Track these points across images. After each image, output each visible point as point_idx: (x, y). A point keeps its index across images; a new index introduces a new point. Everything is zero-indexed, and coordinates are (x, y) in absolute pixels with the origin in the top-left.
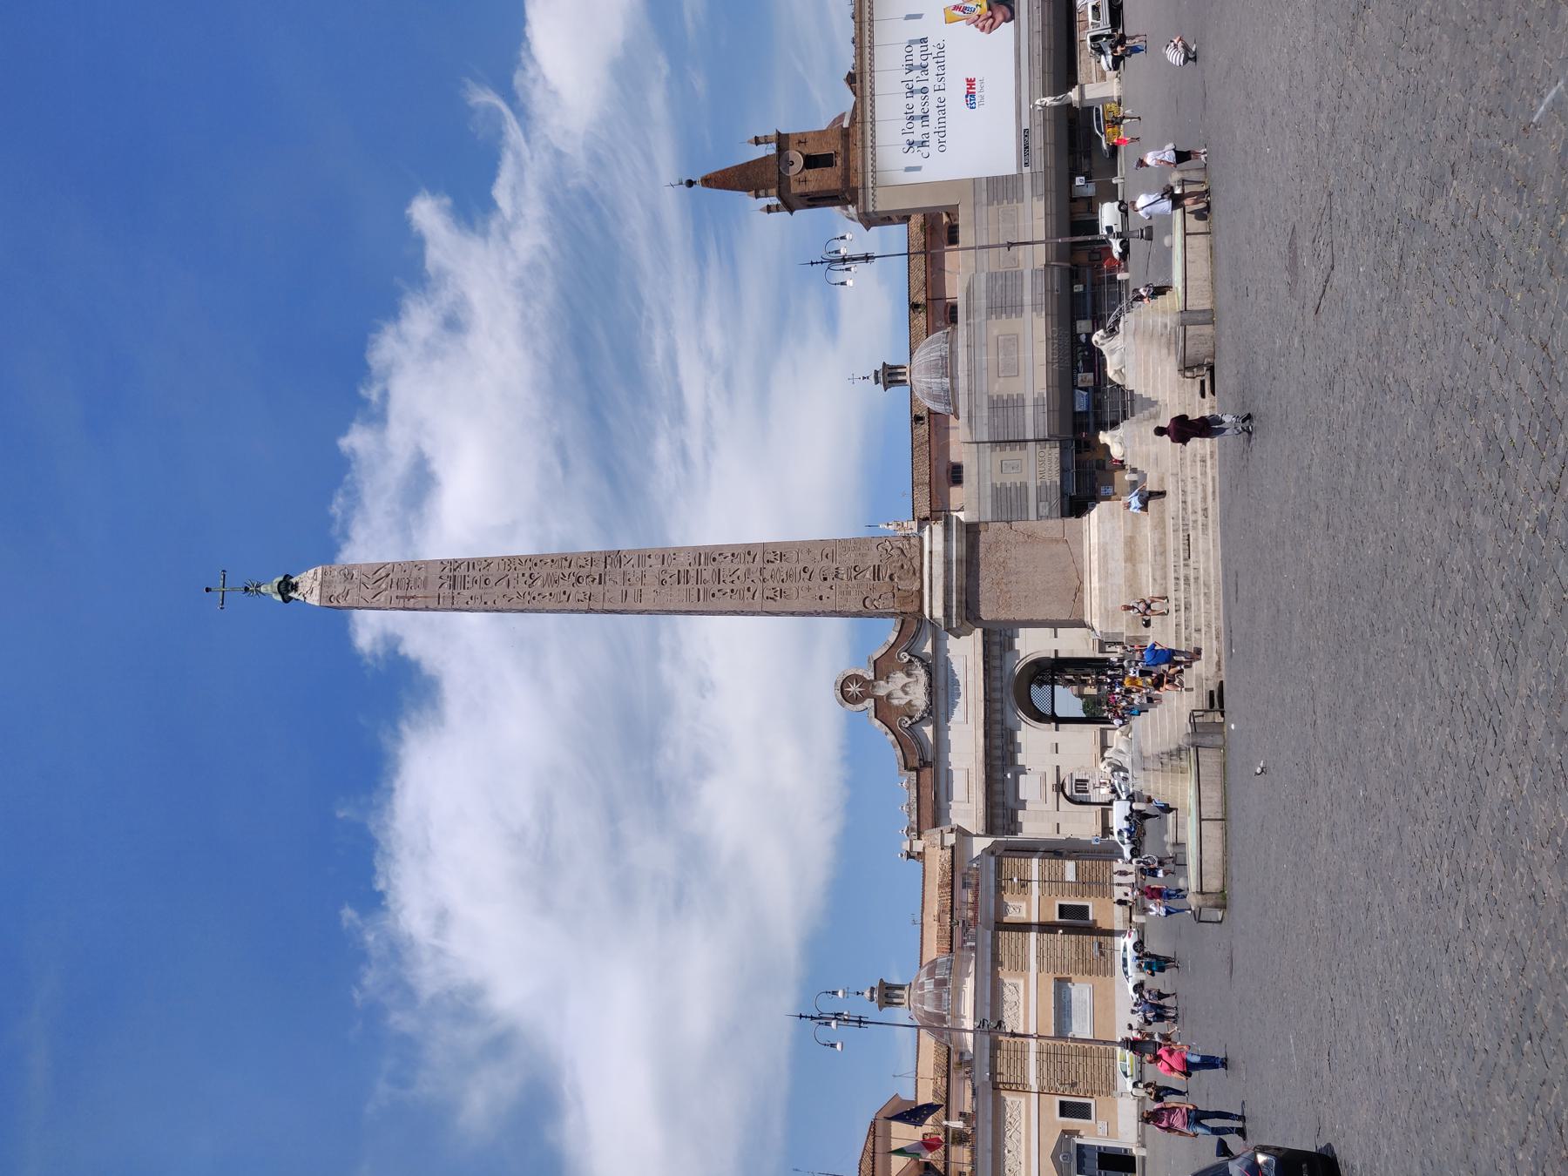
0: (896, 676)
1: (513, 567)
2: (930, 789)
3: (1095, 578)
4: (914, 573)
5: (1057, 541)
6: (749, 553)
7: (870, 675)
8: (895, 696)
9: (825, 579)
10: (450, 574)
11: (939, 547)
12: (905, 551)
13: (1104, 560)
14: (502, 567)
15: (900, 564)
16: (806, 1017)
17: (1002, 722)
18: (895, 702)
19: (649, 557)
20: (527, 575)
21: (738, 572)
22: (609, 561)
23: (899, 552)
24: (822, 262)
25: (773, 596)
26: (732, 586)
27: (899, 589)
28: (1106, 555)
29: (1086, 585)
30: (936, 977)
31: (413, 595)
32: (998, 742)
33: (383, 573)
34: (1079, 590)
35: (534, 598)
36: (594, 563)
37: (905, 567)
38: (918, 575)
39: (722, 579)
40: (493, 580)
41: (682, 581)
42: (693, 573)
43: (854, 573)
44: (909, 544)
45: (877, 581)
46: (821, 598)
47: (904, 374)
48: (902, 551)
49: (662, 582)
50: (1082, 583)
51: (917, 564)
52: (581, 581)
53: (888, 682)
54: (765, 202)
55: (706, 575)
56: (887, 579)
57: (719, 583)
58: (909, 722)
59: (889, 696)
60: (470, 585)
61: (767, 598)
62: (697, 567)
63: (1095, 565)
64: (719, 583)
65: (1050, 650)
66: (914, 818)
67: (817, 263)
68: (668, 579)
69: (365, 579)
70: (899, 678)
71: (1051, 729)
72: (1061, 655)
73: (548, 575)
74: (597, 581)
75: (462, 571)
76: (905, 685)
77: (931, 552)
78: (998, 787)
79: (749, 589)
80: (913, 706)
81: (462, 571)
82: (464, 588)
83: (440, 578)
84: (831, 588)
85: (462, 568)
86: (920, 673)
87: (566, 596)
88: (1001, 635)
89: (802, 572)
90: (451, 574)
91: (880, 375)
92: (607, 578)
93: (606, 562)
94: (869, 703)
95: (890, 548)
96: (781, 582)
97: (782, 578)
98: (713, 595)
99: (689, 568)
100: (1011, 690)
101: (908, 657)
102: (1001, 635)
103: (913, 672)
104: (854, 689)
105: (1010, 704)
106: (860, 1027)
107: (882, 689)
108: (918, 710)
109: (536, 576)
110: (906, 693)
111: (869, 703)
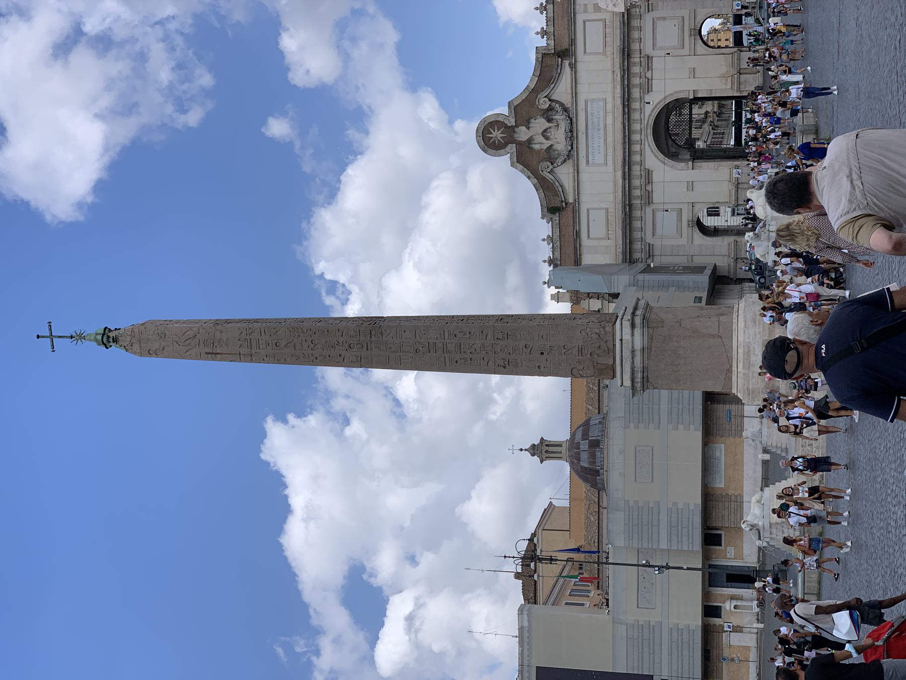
0: (537, 121)
1: (297, 334)
2: (572, 228)
3: (741, 365)
5: (714, 336)
7: (512, 122)
8: (536, 141)
9: (542, 354)
10: (246, 337)
11: (627, 336)
12: (601, 336)
13: (748, 353)
17: (641, 163)
18: (537, 147)
21: (475, 346)
22: (373, 333)
23: (596, 336)
26: (471, 356)
27: (597, 363)
28: (749, 351)
29: (734, 368)
30: (590, 438)
31: (218, 352)
32: (636, 182)
33: (190, 333)
34: (729, 371)
38: (611, 354)
40: (284, 343)
41: (432, 351)
42: (440, 345)
44: (605, 331)
46: (539, 367)
50: (731, 366)
52: (352, 347)
53: (528, 128)
55: (451, 347)
56: (589, 356)
58: (551, 167)
59: (530, 141)
60: (264, 346)
63: (741, 356)
65: (689, 91)
68: (420, 348)
69: (176, 338)
70: (539, 124)
71: (688, 169)
72: (700, 95)
74: (365, 346)
76: (545, 131)
77: (621, 340)
78: (637, 224)
80: (555, 150)
83: (239, 340)
86: (559, 117)
88: (641, 77)
89: (524, 348)
92: (373, 346)
93: (371, 334)
94: (512, 148)
95: (591, 333)
100: (650, 131)
101: (548, 103)
102: (641, 77)
103: (553, 117)
104: (497, 134)
105: (649, 145)
106: (551, 563)
107: (523, 134)
108: (559, 155)
109: (317, 342)
110: (547, 138)
111: (512, 148)
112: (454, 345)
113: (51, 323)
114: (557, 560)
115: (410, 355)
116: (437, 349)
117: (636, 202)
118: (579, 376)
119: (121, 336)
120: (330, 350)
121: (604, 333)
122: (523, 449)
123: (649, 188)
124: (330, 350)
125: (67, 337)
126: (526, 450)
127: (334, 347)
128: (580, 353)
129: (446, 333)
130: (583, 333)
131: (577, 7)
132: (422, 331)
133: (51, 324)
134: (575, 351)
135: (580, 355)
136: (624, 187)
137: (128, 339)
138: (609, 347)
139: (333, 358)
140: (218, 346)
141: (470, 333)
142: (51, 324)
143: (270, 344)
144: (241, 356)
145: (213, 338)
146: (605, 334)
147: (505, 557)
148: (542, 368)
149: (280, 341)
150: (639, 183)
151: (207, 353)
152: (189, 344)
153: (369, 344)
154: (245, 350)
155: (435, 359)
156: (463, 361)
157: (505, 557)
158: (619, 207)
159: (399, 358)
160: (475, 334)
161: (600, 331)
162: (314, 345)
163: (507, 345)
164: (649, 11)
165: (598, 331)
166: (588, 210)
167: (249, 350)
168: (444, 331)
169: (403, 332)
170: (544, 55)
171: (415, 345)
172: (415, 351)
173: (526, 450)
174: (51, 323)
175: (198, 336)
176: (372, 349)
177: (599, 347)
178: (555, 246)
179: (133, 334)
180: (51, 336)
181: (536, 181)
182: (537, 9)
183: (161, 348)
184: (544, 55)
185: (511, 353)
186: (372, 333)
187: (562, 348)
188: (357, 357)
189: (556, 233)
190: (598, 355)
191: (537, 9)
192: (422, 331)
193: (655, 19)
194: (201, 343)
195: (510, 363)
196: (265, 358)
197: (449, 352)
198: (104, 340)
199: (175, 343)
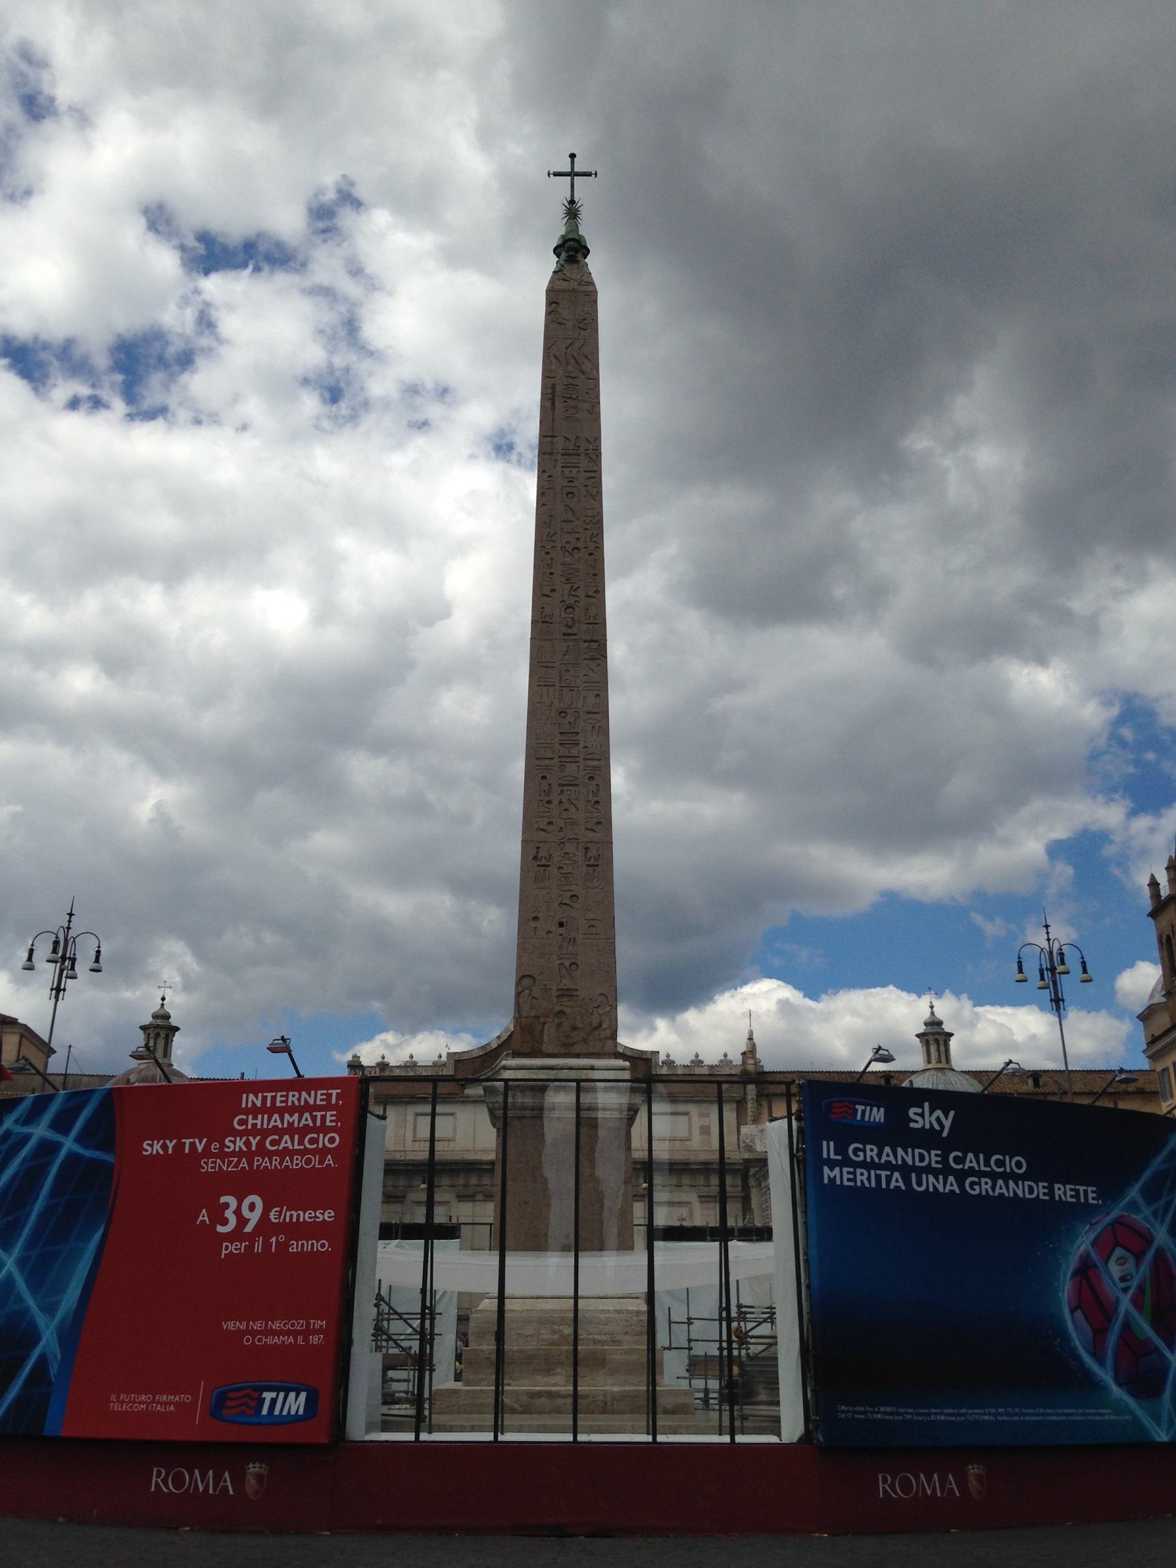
1: (588, 527)
4: (565, 1045)
6: (598, 823)
12: (596, 1033)
14: (589, 513)
15: (579, 1025)
16: (70, 921)
19: (597, 695)
20: (580, 545)
21: (573, 810)
22: (594, 645)
23: (595, 1022)
24: (1049, 940)
25: (540, 855)
26: (556, 802)
27: (544, 1024)
31: (557, 404)
33: (587, 366)
35: (547, 553)
36: (591, 626)
37: (575, 1033)
38: (562, 1051)
39: (565, 788)
42: (574, 752)
43: (567, 964)
44: (606, 1038)
45: (556, 994)
46: (536, 918)
47: (940, 1062)
48: (597, 1028)
49: (562, 713)
51: (576, 1049)
52: (568, 611)
54: (1163, 879)
55: (571, 769)
56: (558, 1008)
57: (560, 785)
61: (538, 848)
62: (582, 756)
64: (560, 785)
66: (397, 1073)
67: (1048, 933)
68: (569, 719)
73: (577, 570)
74: (570, 631)
75: (584, 463)
79: (550, 823)
81: (584, 463)
82: (562, 467)
83: (577, 437)
84: (549, 932)
85: (590, 464)
87: (548, 593)
89: (573, 893)
90: (582, 450)
91: (936, 1029)
92: (571, 644)
93: (592, 641)
96: (558, 865)
97: (564, 867)
98: (544, 778)
99: (581, 746)
106: (52, 990)
112: (575, 774)
113: (596, 176)
114: (57, 998)
115: (556, 702)
116: (567, 746)
117: (461, 1181)
118: (520, 989)
119: (578, 268)
120: (562, 575)
121: (602, 1036)
122: (164, 1002)
123: (480, 1197)
124: (562, 575)
125: (572, 195)
126: (162, 1005)
127: (568, 582)
128: (565, 992)
129: (595, 763)
130: (600, 999)
131: (705, 1105)
132: (599, 724)
133: (594, 176)
134: (567, 983)
135: (559, 993)
136: (481, 1162)
137: (574, 277)
138: (575, 1046)
139: (548, 579)
140: (566, 404)
141: (597, 802)
142: (594, 176)
143: (570, 484)
144: (550, 439)
145: (580, 398)
146: (600, 1040)
147: (71, 915)
148: (533, 924)
149: (576, 498)
150: (485, 1183)
151: (554, 386)
152: (568, 363)
153: (574, 637)
154: (560, 444)
155: (549, 741)
156: (546, 788)
157: (71, 915)
158: (458, 1157)
159: (550, 684)
160: (595, 811)
161: (605, 1030)
162: (571, 551)
163: (577, 864)
164: (700, 1197)
165: (604, 1026)
166: (453, 1114)
167: (561, 451)
168: (600, 760)
169: (596, 693)
170: (648, 1061)
171: (575, 710)
172: (563, 710)
173: (162, 1005)
174: (596, 176)
175: (582, 376)
176: (565, 640)
177: (575, 1028)
178: (409, 1069)
179: (583, 283)
180: (572, 174)
181: (494, 1046)
182: (697, 1056)
183: (561, 320)
184: (648, 1061)
185: (561, 871)
186: (593, 643)
187: (572, 961)
188: (551, 616)
189: (426, 1070)
190: (559, 1025)
191: (697, 1056)
192: (599, 724)
193: (690, 1205)
194: (570, 381)
195: (542, 868)
196: (548, 474)
197: (562, 767)
198: (572, 243)
199: (570, 342)
